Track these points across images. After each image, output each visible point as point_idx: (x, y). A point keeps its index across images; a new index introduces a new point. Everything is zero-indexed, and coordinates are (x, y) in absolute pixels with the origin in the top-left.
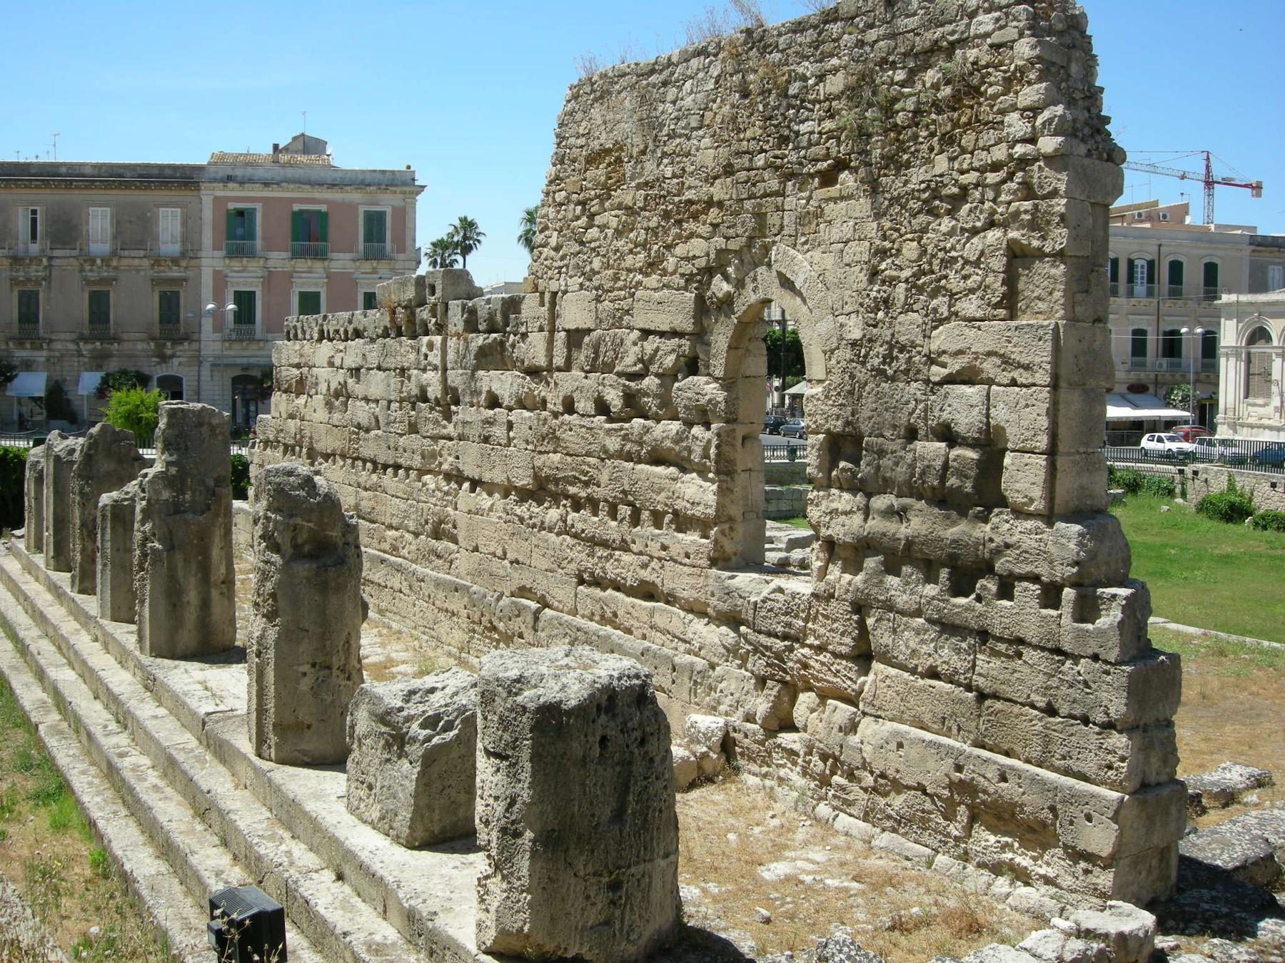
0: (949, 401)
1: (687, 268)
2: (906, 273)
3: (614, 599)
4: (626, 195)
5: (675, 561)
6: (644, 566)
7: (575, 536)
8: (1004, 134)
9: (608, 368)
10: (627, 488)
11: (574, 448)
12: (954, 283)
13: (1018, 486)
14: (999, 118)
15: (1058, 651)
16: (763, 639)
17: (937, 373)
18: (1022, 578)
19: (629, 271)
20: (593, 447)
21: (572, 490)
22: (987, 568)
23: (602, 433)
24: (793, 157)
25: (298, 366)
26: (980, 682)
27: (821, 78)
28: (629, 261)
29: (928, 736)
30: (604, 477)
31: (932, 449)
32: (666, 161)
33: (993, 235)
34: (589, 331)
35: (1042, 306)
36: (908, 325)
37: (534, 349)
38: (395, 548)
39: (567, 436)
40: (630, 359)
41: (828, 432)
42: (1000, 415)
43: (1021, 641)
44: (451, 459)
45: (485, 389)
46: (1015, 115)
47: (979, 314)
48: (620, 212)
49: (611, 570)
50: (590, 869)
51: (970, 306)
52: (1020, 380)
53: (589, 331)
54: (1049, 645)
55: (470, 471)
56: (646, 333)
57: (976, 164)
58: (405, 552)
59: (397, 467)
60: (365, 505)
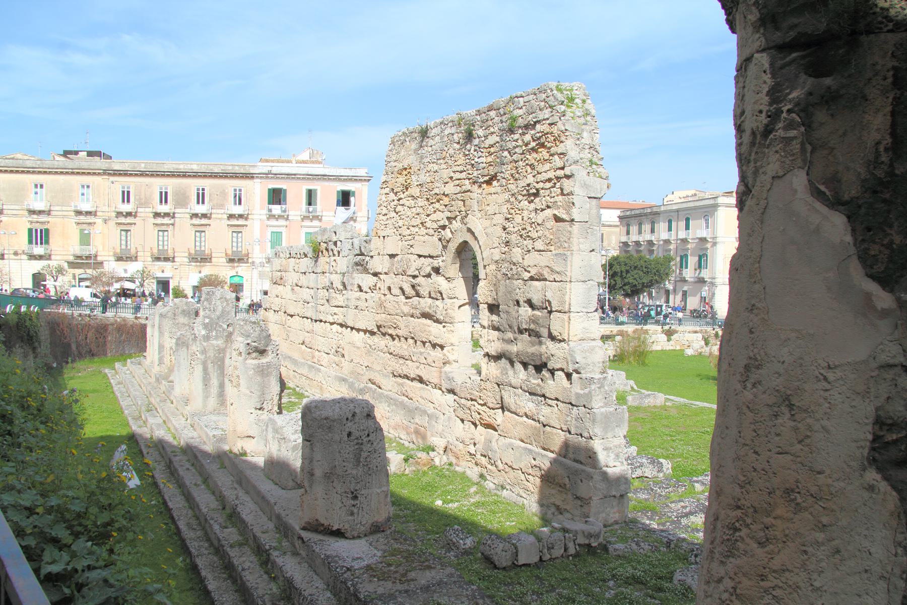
0: (532, 288)
1: (435, 226)
2: (516, 229)
3: (405, 383)
4: (414, 191)
5: (429, 365)
6: (418, 368)
7: (391, 354)
8: (552, 165)
9: (404, 273)
10: (411, 330)
11: (392, 312)
12: (534, 235)
13: (555, 328)
14: (551, 158)
15: (571, 403)
16: (463, 401)
17: (526, 276)
18: (558, 370)
19: (413, 226)
20: (399, 311)
21: (390, 331)
22: (545, 365)
23: (402, 304)
24: (475, 174)
25: (280, 271)
26: (542, 419)
27: (486, 137)
28: (414, 223)
29: (523, 445)
30: (402, 325)
31: (525, 311)
32: (427, 174)
33: (548, 211)
34: (397, 255)
35: (566, 245)
36: (517, 253)
37: (377, 264)
38: (319, 361)
39: (388, 305)
40: (413, 269)
41: (487, 303)
42: (549, 296)
43: (557, 399)
44: (342, 317)
45: (356, 283)
46: (556, 157)
47: (542, 248)
48: (410, 199)
49: (405, 371)
50: (343, 491)
51: (539, 245)
52: (557, 279)
53: (397, 255)
54: (567, 401)
55: (350, 324)
56: (420, 256)
57: (542, 179)
58: (322, 363)
59: (321, 321)
60: (307, 341)
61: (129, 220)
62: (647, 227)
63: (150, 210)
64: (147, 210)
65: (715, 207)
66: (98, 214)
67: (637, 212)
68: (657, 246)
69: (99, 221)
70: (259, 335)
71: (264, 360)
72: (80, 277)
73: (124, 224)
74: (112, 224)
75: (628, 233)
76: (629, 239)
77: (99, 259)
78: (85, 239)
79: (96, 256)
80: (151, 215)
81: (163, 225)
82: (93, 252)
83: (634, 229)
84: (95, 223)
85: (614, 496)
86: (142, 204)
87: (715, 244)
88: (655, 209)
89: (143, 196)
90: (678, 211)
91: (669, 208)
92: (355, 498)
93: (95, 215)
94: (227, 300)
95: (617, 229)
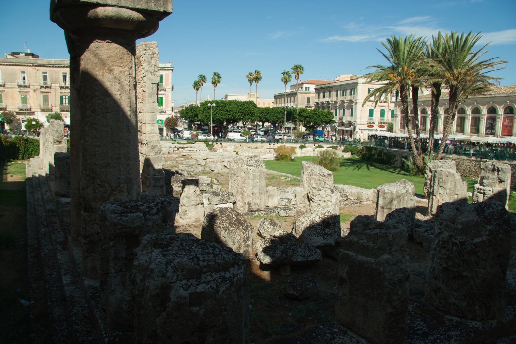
61: (47, 90)
62: (327, 94)
63: (58, 85)
64: (56, 85)
65: (357, 83)
66: (31, 87)
67: (323, 86)
68: (331, 104)
69: (31, 91)
70: (58, 135)
71: (61, 145)
72: (23, 120)
73: (45, 92)
74: (38, 92)
75: (319, 98)
76: (319, 100)
77: (33, 110)
78: (24, 100)
79: (31, 109)
80: (59, 88)
81: (65, 93)
82: (29, 107)
83: (321, 95)
84: (29, 92)
85: (158, 186)
86: (54, 82)
87: (356, 103)
88: (331, 85)
89: (54, 78)
90: (341, 86)
91: (337, 84)
92: (69, 184)
93: (29, 87)
94: (60, 125)
95: (314, 95)
